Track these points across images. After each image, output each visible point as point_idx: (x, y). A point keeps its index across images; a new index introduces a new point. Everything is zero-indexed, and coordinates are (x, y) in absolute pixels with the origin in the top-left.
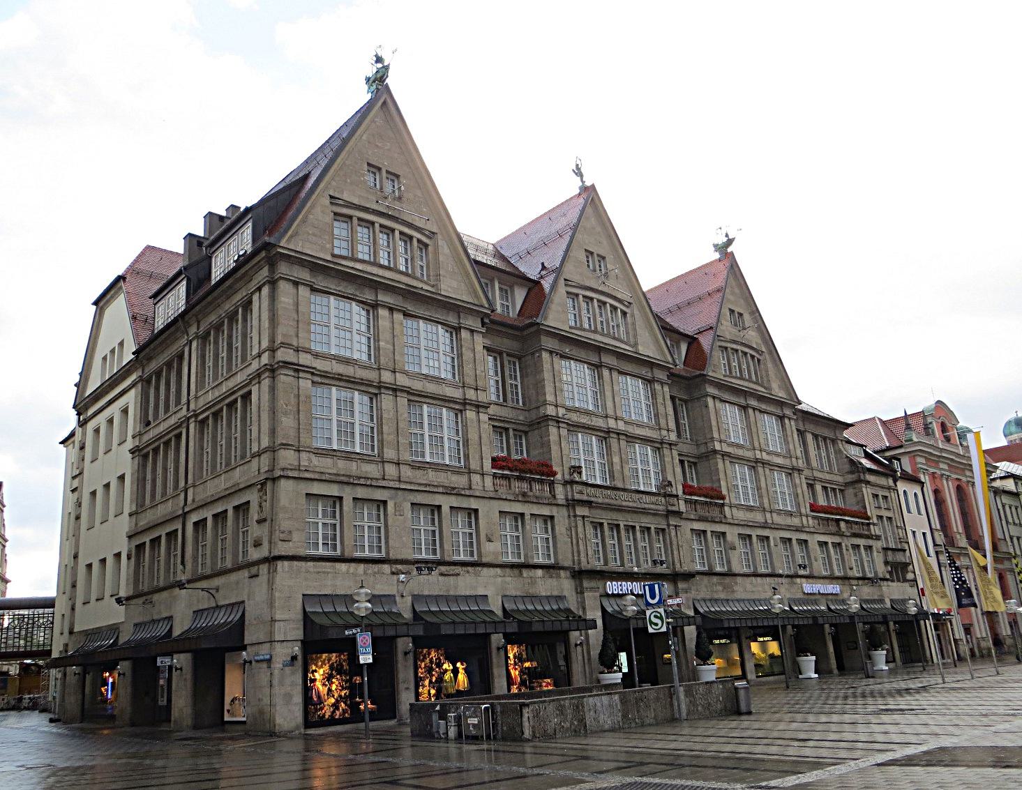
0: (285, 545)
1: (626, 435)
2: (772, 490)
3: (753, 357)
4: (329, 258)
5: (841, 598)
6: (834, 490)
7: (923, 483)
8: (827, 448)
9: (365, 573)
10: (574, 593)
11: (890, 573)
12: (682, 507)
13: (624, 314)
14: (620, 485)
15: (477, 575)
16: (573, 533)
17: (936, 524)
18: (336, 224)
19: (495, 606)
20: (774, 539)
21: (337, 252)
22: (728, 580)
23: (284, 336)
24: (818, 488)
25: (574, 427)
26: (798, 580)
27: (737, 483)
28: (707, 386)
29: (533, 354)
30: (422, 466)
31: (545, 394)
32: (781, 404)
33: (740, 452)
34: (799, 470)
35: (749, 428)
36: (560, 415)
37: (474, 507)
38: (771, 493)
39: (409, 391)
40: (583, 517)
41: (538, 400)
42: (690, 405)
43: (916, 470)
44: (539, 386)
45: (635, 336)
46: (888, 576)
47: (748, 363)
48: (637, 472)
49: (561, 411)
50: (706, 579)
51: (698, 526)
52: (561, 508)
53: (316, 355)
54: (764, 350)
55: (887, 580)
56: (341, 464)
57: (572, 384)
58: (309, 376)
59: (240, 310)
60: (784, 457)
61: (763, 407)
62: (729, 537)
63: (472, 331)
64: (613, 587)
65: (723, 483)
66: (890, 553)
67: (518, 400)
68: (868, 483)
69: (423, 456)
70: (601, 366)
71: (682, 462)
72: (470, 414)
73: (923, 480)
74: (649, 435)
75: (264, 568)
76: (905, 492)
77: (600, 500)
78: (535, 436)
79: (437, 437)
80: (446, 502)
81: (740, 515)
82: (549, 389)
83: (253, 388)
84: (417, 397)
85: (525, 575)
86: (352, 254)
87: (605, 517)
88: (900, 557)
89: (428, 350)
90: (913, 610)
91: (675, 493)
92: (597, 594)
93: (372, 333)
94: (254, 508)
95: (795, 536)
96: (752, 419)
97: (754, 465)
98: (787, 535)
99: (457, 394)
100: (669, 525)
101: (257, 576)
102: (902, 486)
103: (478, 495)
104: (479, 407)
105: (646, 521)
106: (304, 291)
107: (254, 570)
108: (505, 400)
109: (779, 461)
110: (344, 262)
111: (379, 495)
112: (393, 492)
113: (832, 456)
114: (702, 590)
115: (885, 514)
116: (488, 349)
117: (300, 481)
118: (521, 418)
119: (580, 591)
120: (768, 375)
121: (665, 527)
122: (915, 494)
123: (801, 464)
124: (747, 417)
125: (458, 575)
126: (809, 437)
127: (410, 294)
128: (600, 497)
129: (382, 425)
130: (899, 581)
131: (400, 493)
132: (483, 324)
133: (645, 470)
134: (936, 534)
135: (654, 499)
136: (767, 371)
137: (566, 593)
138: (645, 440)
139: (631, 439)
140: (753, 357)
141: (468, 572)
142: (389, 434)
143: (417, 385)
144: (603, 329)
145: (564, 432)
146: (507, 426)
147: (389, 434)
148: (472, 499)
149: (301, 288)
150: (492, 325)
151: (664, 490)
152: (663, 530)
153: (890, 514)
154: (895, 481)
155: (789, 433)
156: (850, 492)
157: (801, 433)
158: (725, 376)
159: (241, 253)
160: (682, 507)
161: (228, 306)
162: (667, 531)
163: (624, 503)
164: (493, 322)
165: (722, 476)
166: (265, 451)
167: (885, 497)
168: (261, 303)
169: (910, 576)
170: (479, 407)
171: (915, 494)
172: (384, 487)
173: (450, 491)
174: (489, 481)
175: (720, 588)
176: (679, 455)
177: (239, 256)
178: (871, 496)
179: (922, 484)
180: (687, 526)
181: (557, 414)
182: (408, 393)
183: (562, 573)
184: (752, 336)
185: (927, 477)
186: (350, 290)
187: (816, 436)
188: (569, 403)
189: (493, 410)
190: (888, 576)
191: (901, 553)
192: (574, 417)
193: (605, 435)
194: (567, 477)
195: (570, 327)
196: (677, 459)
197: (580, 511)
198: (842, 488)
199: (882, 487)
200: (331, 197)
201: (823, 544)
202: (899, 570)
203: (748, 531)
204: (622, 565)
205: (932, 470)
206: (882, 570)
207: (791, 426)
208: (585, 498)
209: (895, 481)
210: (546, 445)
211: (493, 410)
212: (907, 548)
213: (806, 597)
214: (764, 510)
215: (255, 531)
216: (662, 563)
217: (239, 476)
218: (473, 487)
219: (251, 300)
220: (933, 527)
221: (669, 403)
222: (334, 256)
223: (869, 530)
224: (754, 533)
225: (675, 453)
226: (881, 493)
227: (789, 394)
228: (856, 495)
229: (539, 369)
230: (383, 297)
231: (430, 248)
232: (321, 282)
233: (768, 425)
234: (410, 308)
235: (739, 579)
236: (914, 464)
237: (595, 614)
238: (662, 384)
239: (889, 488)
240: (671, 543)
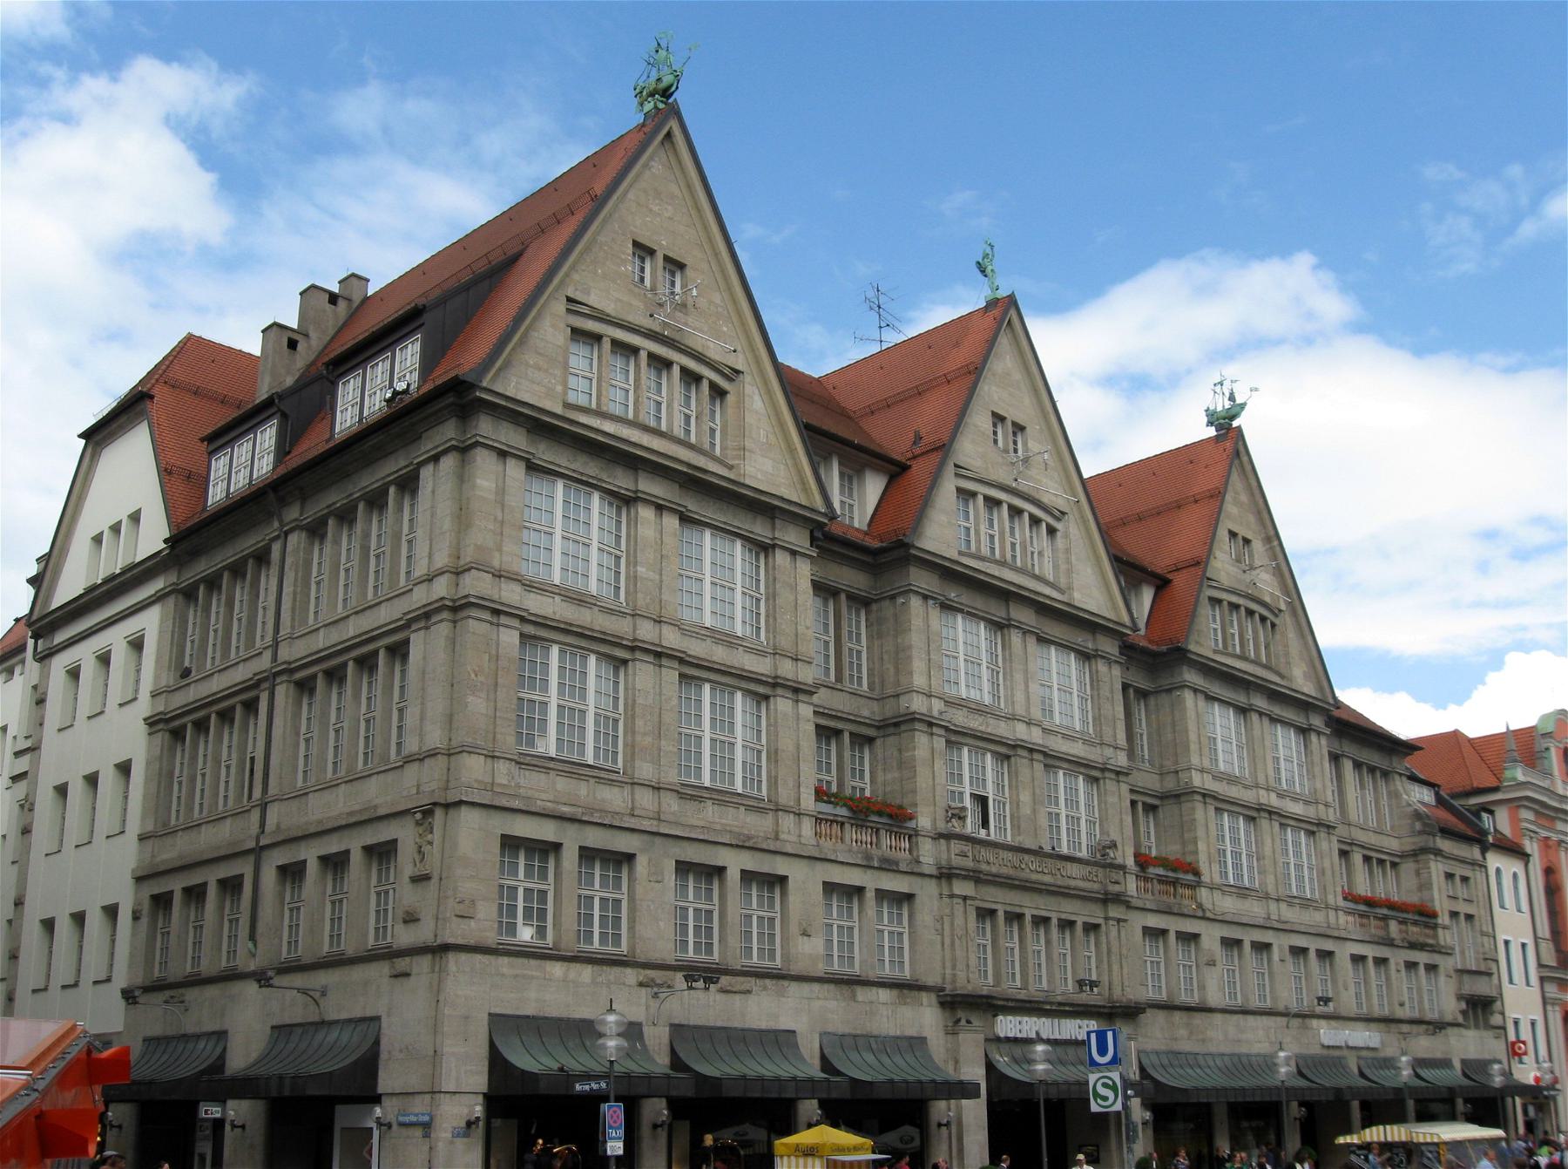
0: (464, 924)
1: (1045, 754)
2: (1281, 860)
3: (1263, 619)
4: (559, 410)
5: (1382, 1054)
6: (1381, 862)
7: (1528, 856)
8: (1375, 789)
9: (594, 982)
10: (942, 1034)
11: (1464, 1013)
12: (1131, 886)
13: (1052, 531)
15: (781, 994)
16: (947, 927)
17: (1544, 930)
18: (574, 348)
19: (810, 1048)
20: (1280, 946)
21: (572, 398)
22: (1198, 1019)
23: (479, 548)
24: (1357, 858)
25: (956, 737)
26: (1315, 1022)
27: (1222, 847)
28: (1185, 668)
29: (893, 598)
30: (692, 794)
31: (911, 673)
32: (1304, 705)
33: (1234, 792)
34: (1329, 827)
35: (1251, 748)
36: (935, 713)
37: (780, 872)
38: (1280, 869)
39: (682, 660)
40: (965, 898)
41: (898, 684)
42: (1152, 701)
43: (1522, 832)
44: (901, 658)
45: (1069, 572)
46: (1460, 1020)
47: (1255, 632)
48: (1058, 821)
49: (937, 706)
50: (1161, 1016)
51: (1154, 921)
52: (927, 881)
53: (529, 586)
54: (1283, 607)
55: (1458, 1025)
56: (562, 784)
57: (957, 658)
58: (516, 623)
59: (392, 490)
60: (1307, 803)
61: (1277, 710)
63: (794, 553)
64: (1008, 1026)
65: (1201, 846)
66: (1466, 978)
67: (860, 678)
68: (1438, 853)
69: (699, 776)
70: (1009, 626)
71: (1133, 803)
72: (783, 705)
73: (1528, 850)
74: (1082, 754)
75: (423, 964)
76: (1498, 871)
77: (994, 870)
78: (886, 747)
79: (729, 741)
80: (735, 863)
81: (1228, 905)
82: (918, 665)
83: (413, 637)
84: (692, 671)
85: (860, 998)
86: (598, 404)
87: (1001, 899)
88: (1481, 987)
89: (718, 587)
90: (1498, 1081)
91: (1119, 861)
92: (981, 1037)
93: (623, 548)
94: (406, 852)
95: (1313, 945)
96: (1257, 732)
97: (1254, 814)
98: (1300, 941)
99: (761, 666)
100: (1107, 919)
101: (407, 975)
102: (1494, 861)
103: (790, 850)
104: (798, 691)
105: (1069, 909)
106: (515, 470)
107: (402, 964)
108: (839, 679)
109: (1297, 809)
110: (583, 419)
111: (623, 843)
112: (646, 837)
113: (1384, 801)
114: (1155, 1035)
115: (1463, 908)
116: (820, 588)
117: (492, 812)
118: (866, 713)
119: (952, 1030)
120: (1287, 654)
121: (1100, 921)
122: (1515, 875)
123: (1331, 816)
124: (1249, 730)
125: (749, 992)
126: (1348, 766)
127: (694, 482)
129: (633, 717)
130: (1477, 1027)
131: (658, 840)
132: (813, 540)
133: (1075, 818)
134: (1543, 945)
136: (1286, 646)
137: (927, 1033)
138: (1077, 765)
139: (1052, 760)
140: (1263, 619)
141: (765, 988)
142: (645, 734)
143: (697, 649)
144: (1014, 557)
145: (940, 743)
146: (840, 725)
147: (645, 734)
148: (779, 859)
149: (511, 462)
150: (829, 541)
151: (1103, 859)
152: (1096, 927)
153: (1470, 910)
154: (1483, 853)
155: (1316, 759)
156: (1408, 867)
157: (1335, 758)
158: (1215, 652)
159: (401, 386)
160: (1131, 886)
161: (368, 480)
162: (1103, 928)
163: (1034, 877)
164: (831, 538)
165: (1200, 833)
166: (433, 754)
167: (1465, 879)
168: (437, 482)
169: (1496, 1020)
170: (798, 691)
171: (1515, 875)
172: (633, 830)
173: (743, 845)
174: (807, 827)
175: (1183, 1032)
176: (1132, 791)
177: (396, 394)
178: (1442, 878)
179: (1524, 856)
180: (1139, 921)
181: (930, 709)
182: (681, 661)
183: (926, 998)
184: (1266, 584)
185: (1535, 846)
186: (589, 467)
187: (1358, 765)
188: (950, 691)
189: (822, 697)
190: (1460, 1020)
191: (1486, 978)
192: (960, 718)
193: (1007, 752)
194: (942, 826)
195: (960, 553)
196: (1127, 797)
197: (962, 888)
198: (1397, 860)
199: (1463, 861)
200: (569, 300)
201: (1358, 959)
202: (1480, 1008)
204: (1025, 987)
205: (1544, 833)
206: (1450, 1007)
207: (1321, 745)
208: (969, 863)
209: (1483, 853)
210: (906, 766)
211: (822, 697)
212: (1494, 970)
213: (1325, 1052)
215: (407, 895)
216: (1093, 984)
217: (377, 794)
218: (782, 836)
219: (417, 478)
220: (1540, 934)
221: (1119, 697)
222: (567, 405)
223: (1435, 937)
225: (1125, 788)
226: (1459, 871)
227: (1321, 689)
228: (1418, 873)
229: (901, 627)
230: (650, 486)
231: (730, 398)
232: (545, 453)
233: (1285, 743)
234: (692, 505)
235: (1218, 1017)
236: (1515, 821)
237: (975, 1073)
238: (1109, 662)
239: (1473, 863)
240: (1109, 951)
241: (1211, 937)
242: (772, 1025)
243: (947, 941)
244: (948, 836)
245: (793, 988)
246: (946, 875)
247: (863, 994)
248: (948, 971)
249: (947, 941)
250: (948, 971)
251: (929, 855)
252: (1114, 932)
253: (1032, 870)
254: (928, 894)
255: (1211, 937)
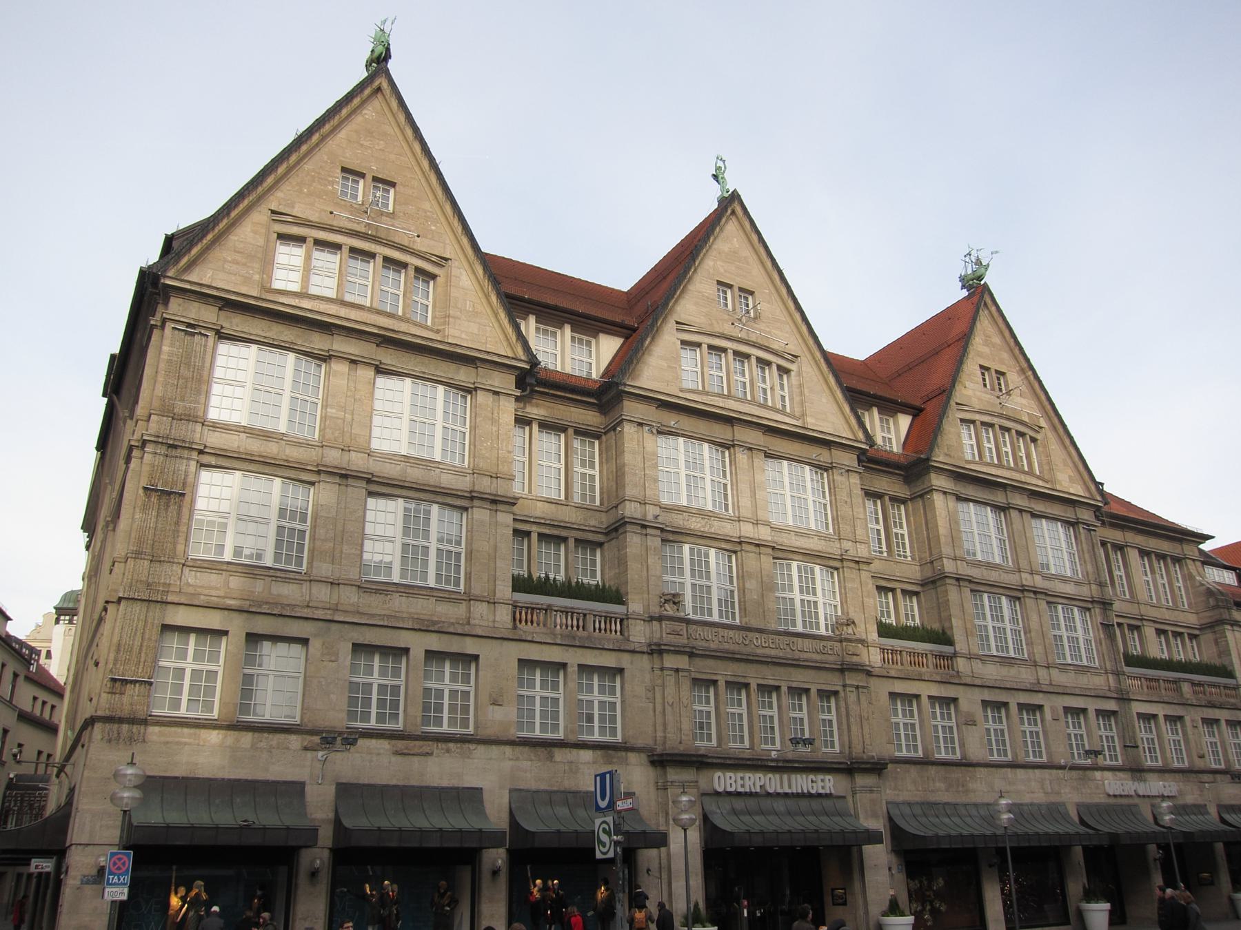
14: (755, 623)
20: (1053, 709)
62: (964, 705)
81: (991, 672)
100: (844, 686)
105: (800, 678)
121: (839, 688)
128: (713, 641)
135: (818, 645)
160: (874, 658)
162: (842, 694)
163: (759, 651)
180: (881, 689)
194: (655, 610)
203: (1002, 697)
214: (1035, 665)
224: (1013, 700)
241: (970, 701)
242: (455, 783)
243: (659, 708)
244: (660, 619)
245: (480, 750)
246: (656, 650)
247: (559, 755)
248: (660, 734)
249: (659, 708)
250: (660, 734)
251: (640, 634)
252: (852, 697)
253: (760, 645)
254: (639, 669)
255: (970, 701)
